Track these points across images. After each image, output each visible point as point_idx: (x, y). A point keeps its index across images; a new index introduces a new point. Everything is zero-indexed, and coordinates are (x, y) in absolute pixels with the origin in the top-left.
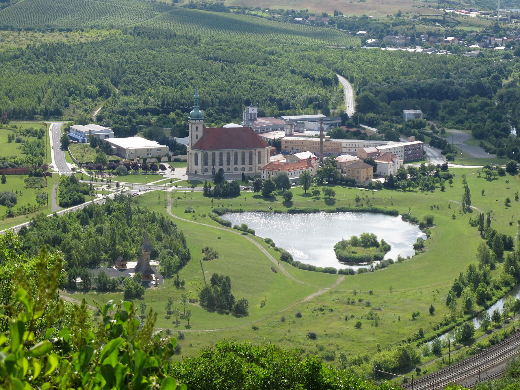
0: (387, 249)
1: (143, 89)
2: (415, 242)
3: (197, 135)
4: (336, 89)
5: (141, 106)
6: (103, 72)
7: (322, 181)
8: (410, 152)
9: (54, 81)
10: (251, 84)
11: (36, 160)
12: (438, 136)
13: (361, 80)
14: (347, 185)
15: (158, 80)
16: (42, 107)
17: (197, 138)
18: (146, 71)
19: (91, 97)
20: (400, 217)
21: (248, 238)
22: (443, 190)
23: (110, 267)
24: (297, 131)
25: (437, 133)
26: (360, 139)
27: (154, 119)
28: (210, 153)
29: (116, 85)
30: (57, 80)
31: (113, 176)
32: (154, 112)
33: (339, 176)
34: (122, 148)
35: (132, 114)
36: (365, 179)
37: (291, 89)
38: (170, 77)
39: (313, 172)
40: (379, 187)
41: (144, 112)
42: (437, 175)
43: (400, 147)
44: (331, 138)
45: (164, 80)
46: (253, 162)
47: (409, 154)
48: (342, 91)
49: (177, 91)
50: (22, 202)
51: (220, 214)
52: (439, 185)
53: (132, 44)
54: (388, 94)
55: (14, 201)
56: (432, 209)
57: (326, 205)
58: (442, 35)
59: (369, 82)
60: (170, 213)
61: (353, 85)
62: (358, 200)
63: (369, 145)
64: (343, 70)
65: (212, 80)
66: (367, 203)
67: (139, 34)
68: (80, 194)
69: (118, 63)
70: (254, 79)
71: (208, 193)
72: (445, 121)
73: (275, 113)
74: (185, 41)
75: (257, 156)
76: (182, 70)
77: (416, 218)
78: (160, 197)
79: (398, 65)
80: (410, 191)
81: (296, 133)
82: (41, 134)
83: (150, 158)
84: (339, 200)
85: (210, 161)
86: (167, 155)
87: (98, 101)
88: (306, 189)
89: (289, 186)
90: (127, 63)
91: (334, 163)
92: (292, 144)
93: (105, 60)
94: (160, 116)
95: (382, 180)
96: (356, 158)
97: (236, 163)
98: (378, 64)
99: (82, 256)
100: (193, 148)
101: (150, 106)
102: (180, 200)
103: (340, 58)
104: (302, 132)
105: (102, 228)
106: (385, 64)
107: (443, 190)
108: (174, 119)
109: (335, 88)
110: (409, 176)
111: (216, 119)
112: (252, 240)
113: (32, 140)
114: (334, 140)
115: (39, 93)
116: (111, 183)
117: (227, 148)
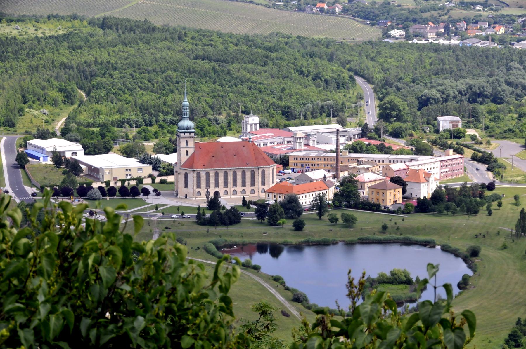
3: (187, 151)
17: (187, 154)
20: (438, 247)
27: (133, 132)
34: (95, 168)
46: (256, 183)
63: (395, 160)
85: (203, 183)
97: (235, 185)
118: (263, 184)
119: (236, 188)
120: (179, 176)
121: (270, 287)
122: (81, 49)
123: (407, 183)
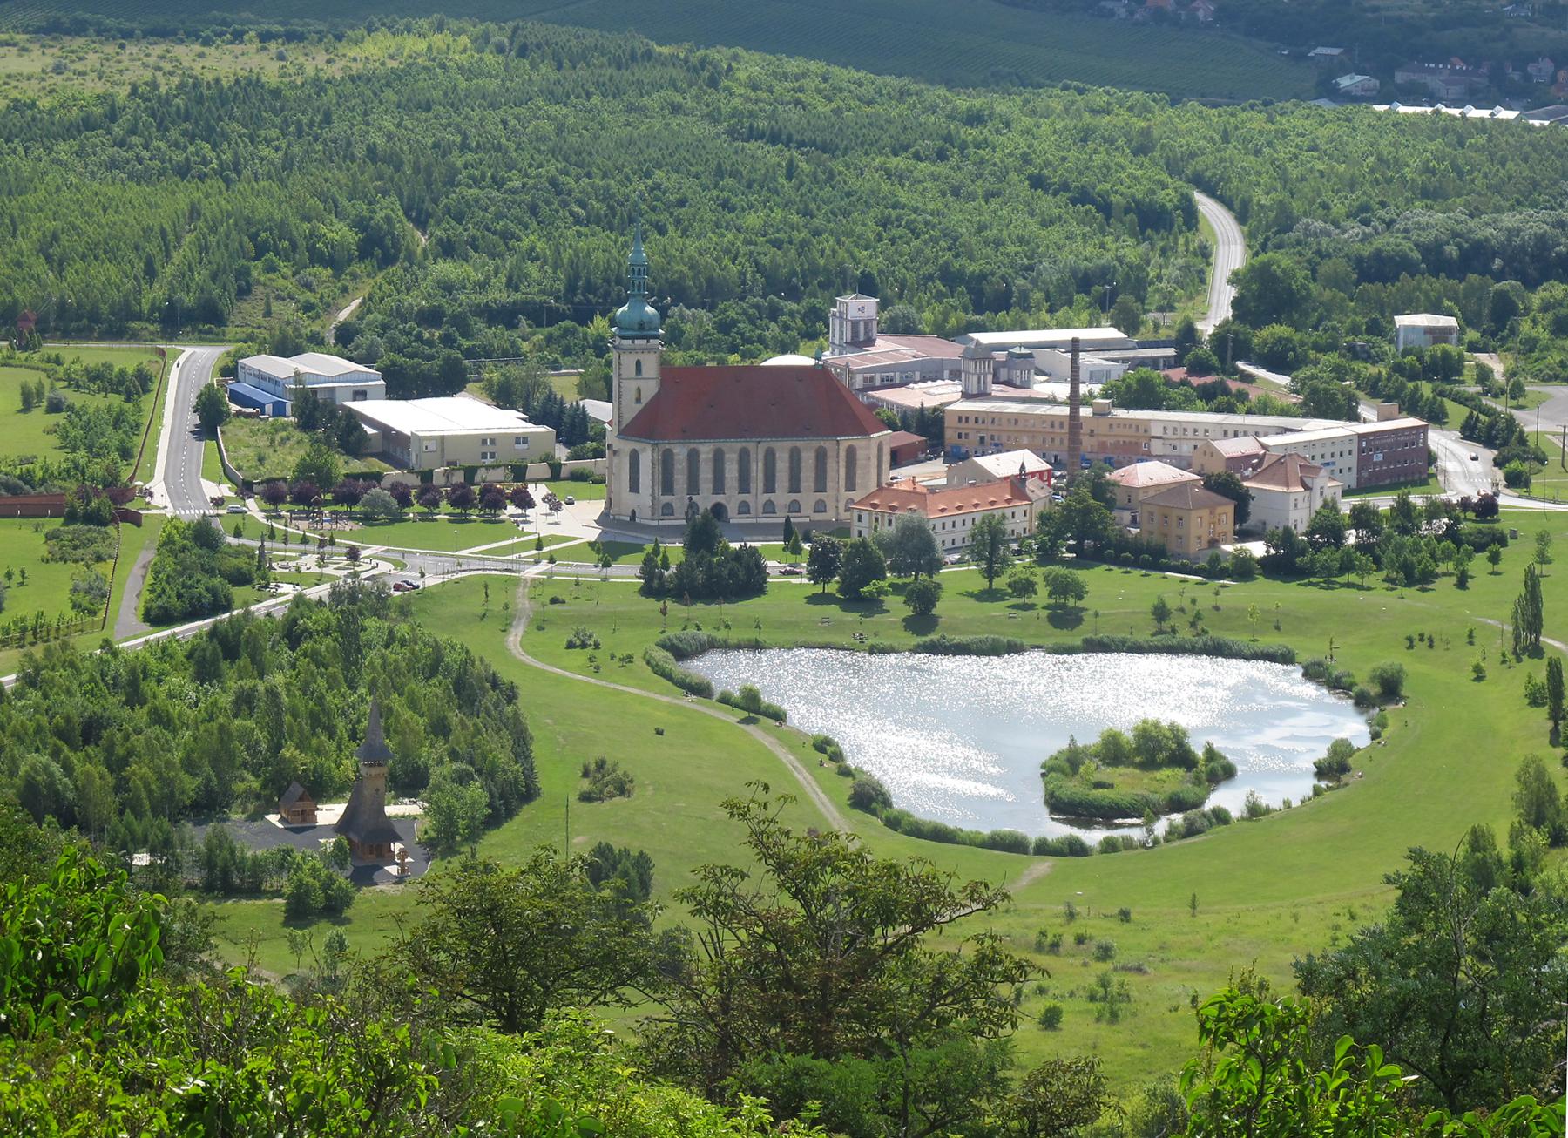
0: (1221, 772)
2: (1322, 753)
3: (639, 390)
4: (1187, 243)
5: (498, 295)
6: (380, 178)
7: (1055, 547)
8: (1378, 457)
9: (209, 208)
11: (97, 468)
12: (1499, 406)
13: (1272, 215)
14: (1137, 564)
15: (565, 205)
16: (155, 294)
17: (638, 400)
18: (527, 175)
22: (1462, 583)
23: (258, 815)
24: (1009, 383)
25: (1496, 396)
26: (1218, 410)
27: (529, 339)
28: (680, 451)
29: (421, 223)
30: (215, 200)
31: (349, 526)
32: (540, 315)
33: (1112, 532)
34: (399, 434)
36: (1205, 544)
37: (1021, 240)
38: (606, 197)
39: (1020, 520)
40: (1243, 570)
41: (505, 316)
42: (1452, 534)
43: (1342, 439)
44: (1114, 406)
45: (582, 205)
46: (830, 485)
47: (1376, 464)
48: (1205, 253)
49: (625, 244)
51: (681, 654)
52: (1450, 566)
53: (492, 85)
54: (1359, 261)
56: (1411, 647)
57: (1050, 629)
59: (1298, 220)
60: (515, 653)
61: (1246, 228)
62: (1161, 613)
63: (1241, 430)
64: (1222, 178)
65: (751, 207)
66: (1193, 625)
67: (523, 52)
68: (217, 581)
69: (436, 146)
71: (655, 584)
72: (1536, 354)
73: (952, 321)
74: (678, 74)
75: (842, 463)
76: (648, 175)
77: (1349, 675)
78: (491, 601)
79: (1415, 162)
80: (1349, 585)
81: (1001, 387)
82: (141, 384)
83: (488, 468)
84: (1097, 615)
85: (680, 480)
86: (548, 458)
87: (354, 276)
88: (991, 574)
89: (934, 565)
91: (1101, 490)
92: (980, 426)
93: (390, 136)
95: (1258, 549)
96: (1188, 476)
97: (770, 487)
98: (1346, 159)
99: (166, 782)
100: (626, 432)
101: (528, 293)
102: (556, 607)
103: (1217, 137)
104: (1025, 385)
105: (254, 689)
106: (1371, 159)
107: (1462, 583)
108: (601, 338)
109: (1181, 241)
110: (1351, 538)
111: (749, 341)
113: (97, 402)
114: (1121, 413)
115: (153, 248)
116: (335, 550)
118: (851, 486)
119: (771, 496)
120: (616, 460)
121: (796, 764)
122: (428, 109)
123: (1251, 493)
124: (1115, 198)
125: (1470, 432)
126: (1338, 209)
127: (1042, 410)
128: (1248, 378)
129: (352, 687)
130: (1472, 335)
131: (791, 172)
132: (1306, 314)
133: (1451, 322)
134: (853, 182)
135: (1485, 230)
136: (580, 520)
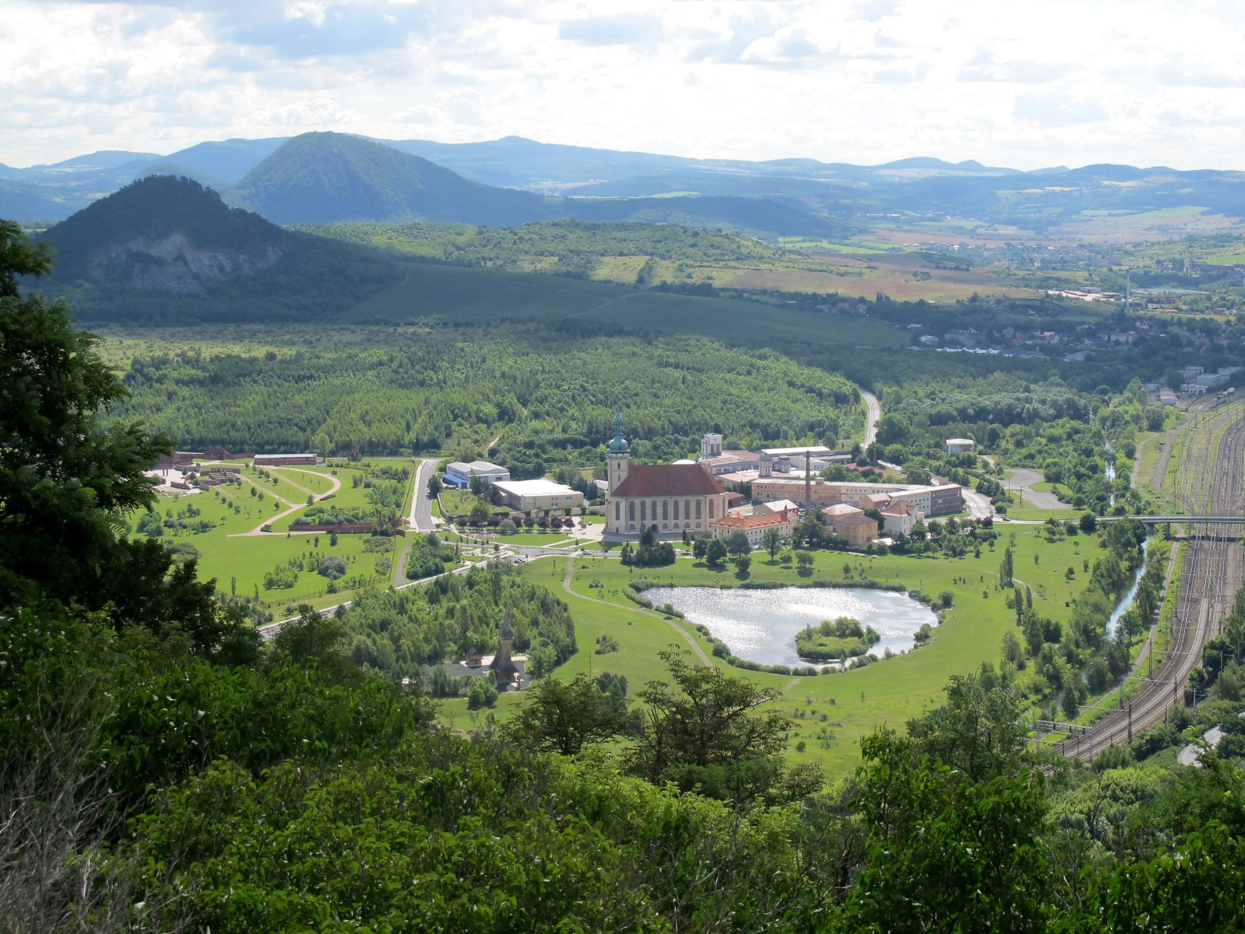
0: (874, 639)
1: (562, 410)
2: (917, 630)
8: (940, 501)
9: (433, 399)
10: (725, 402)
11: (386, 511)
12: (992, 478)
14: (835, 549)
16: (409, 437)
19: (485, 421)
21: (673, 624)
22: (977, 556)
23: (457, 662)
24: (780, 471)
27: (572, 454)
28: (637, 502)
29: (525, 405)
31: (494, 536)
32: (577, 444)
35: (541, 447)
37: (784, 409)
38: (605, 392)
39: (785, 530)
40: (882, 551)
41: (561, 444)
42: (972, 534)
48: (864, 414)
50: (352, 572)
51: (638, 590)
52: (972, 548)
54: (930, 416)
55: (341, 570)
58: (1036, 329)
60: (567, 591)
62: (847, 570)
70: (729, 395)
78: (557, 568)
82: (404, 475)
85: (638, 514)
86: (580, 506)
88: (772, 554)
89: (748, 550)
90: (543, 371)
91: (820, 517)
94: (583, 450)
95: (888, 541)
97: (676, 518)
99: (417, 648)
100: (613, 494)
104: (787, 472)
105: (454, 607)
107: (977, 556)
108: (602, 453)
112: (677, 628)
113: (385, 483)
114: (828, 483)
115: (409, 417)
117: (663, 494)
118: (711, 516)
124: (825, 391)
125: (980, 490)
126: (921, 393)
127: (794, 482)
128: (883, 467)
129: (497, 605)
130: (980, 448)
131: (684, 379)
132: (908, 439)
133: (971, 442)
134: (711, 385)
135: (985, 402)
136: (594, 532)
